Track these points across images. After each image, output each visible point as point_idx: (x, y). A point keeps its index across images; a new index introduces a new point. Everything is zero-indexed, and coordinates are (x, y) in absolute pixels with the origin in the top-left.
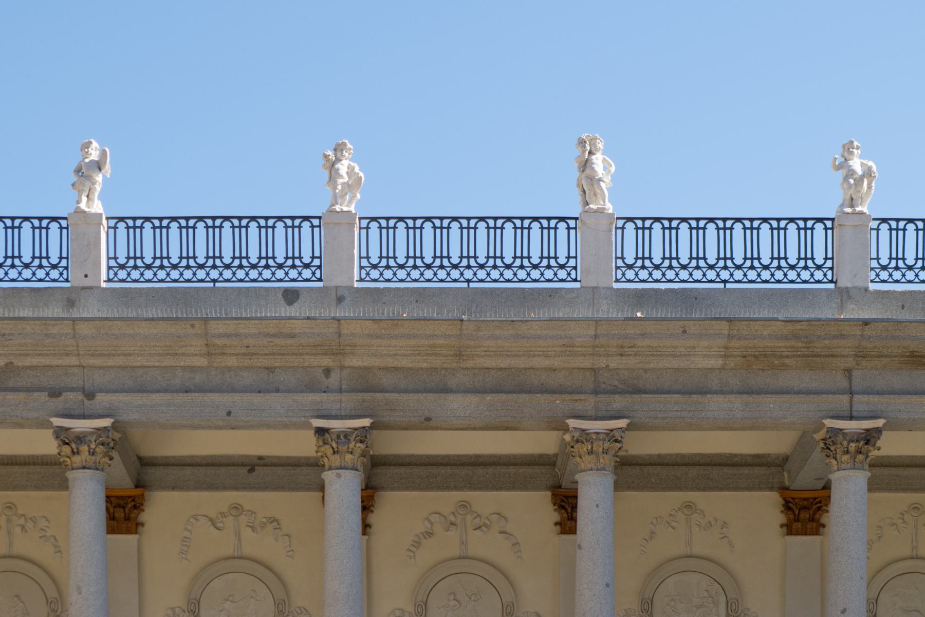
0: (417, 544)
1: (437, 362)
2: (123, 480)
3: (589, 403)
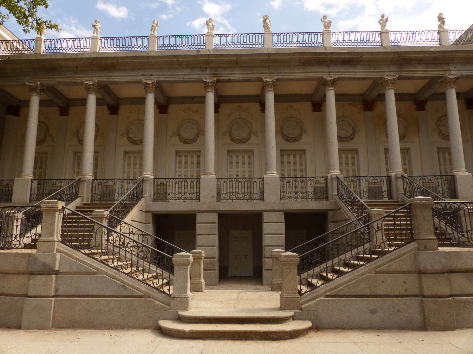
0: (229, 115)
2: (162, 101)
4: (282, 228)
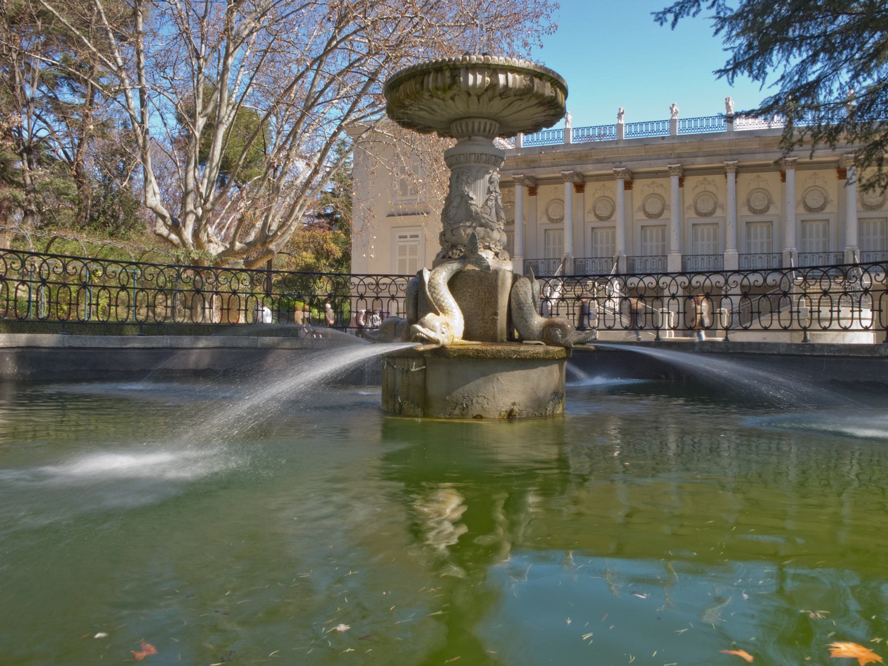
0: (694, 189)
1: (695, 150)
3: (729, 157)
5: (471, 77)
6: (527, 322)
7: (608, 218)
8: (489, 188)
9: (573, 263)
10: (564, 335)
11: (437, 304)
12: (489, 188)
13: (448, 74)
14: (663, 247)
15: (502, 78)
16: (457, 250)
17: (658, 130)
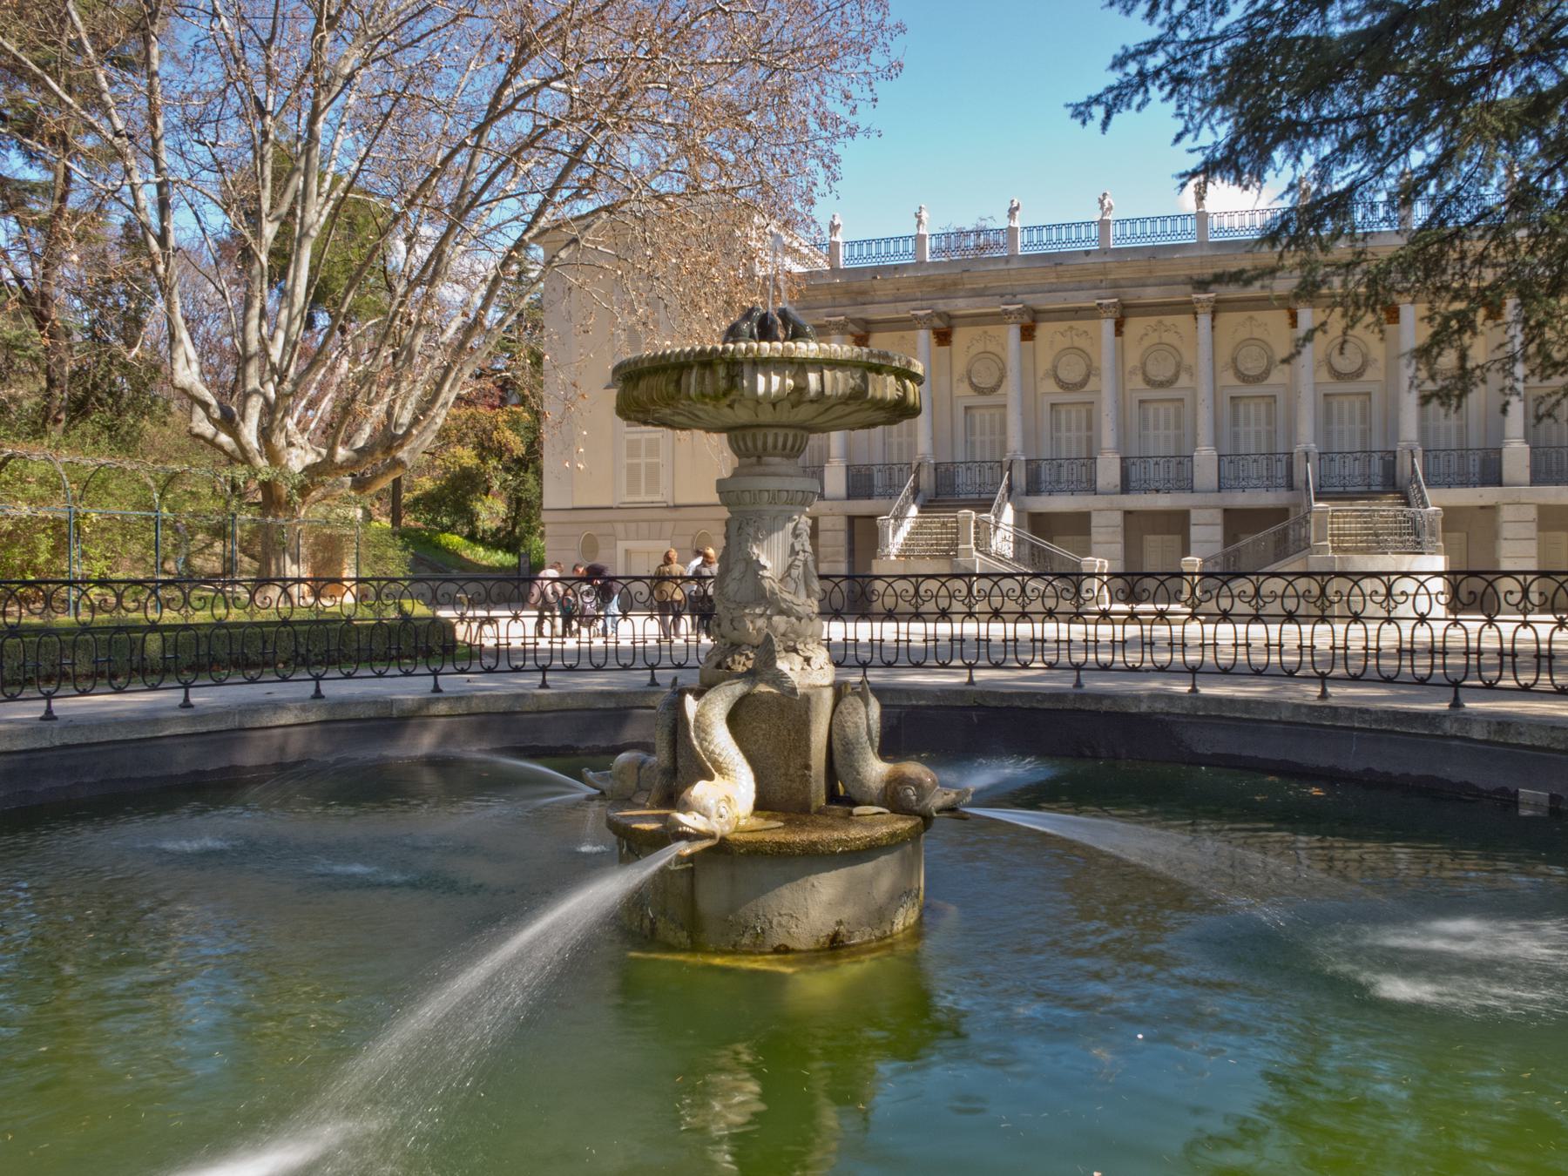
1: (1142, 275)
4: (1217, 533)
5: (761, 380)
6: (858, 773)
7: (993, 390)
8: (793, 546)
9: (932, 471)
10: (921, 798)
11: (709, 759)
12: (793, 546)
13: (722, 371)
14: (1089, 440)
15: (813, 378)
16: (741, 654)
17: (1078, 239)
